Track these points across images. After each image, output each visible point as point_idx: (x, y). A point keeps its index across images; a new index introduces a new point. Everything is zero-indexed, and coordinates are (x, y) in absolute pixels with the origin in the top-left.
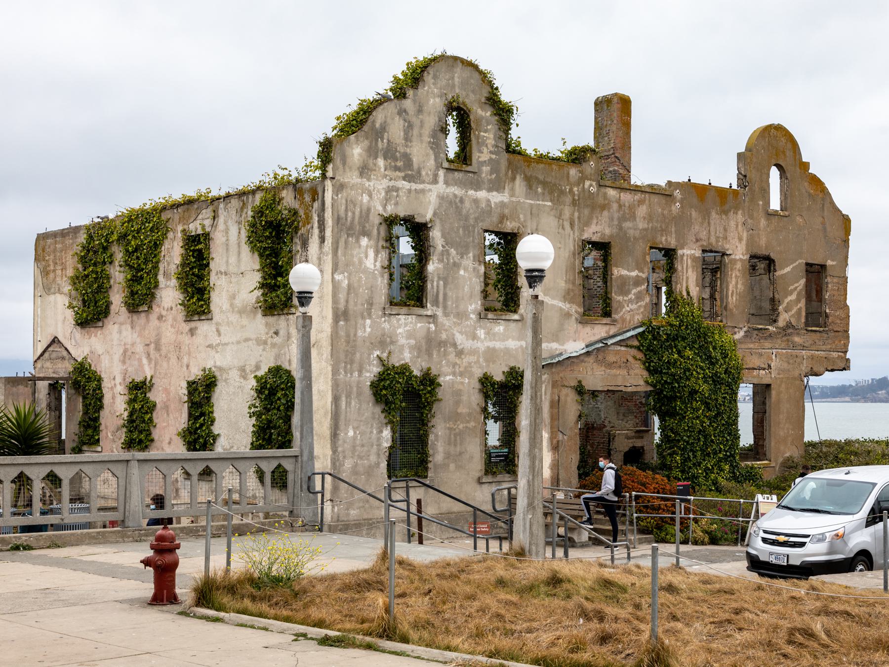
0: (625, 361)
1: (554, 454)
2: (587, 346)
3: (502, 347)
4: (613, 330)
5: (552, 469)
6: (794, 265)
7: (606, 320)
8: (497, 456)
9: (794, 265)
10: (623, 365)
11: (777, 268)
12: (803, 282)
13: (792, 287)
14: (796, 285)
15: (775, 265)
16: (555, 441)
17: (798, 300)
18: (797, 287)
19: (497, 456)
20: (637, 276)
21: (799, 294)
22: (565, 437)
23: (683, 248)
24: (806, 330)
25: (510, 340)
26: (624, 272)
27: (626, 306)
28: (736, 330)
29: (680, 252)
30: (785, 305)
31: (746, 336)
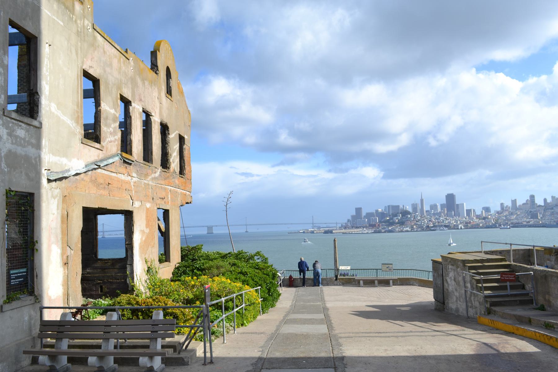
0: (108, 184)
1: (64, 270)
2: (86, 166)
3: (23, 153)
4: (101, 155)
5: (63, 286)
6: (175, 133)
7: (97, 145)
8: (17, 278)
9: (175, 133)
10: (106, 187)
11: (170, 132)
12: (178, 145)
13: (175, 147)
14: (176, 146)
15: (168, 131)
16: (65, 257)
17: (177, 156)
18: (176, 148)
19: (17, 278)
20: (114, 114)
21: (177, 153)
22: (72, 252)
23: (134, 103)
24: (180, 176)
25: (30, 147)
26: (107, 108)
27: (108, 136)
28: (156, 170)
29: (133, 104)
30: (173, 158)
31: (160, 175)
